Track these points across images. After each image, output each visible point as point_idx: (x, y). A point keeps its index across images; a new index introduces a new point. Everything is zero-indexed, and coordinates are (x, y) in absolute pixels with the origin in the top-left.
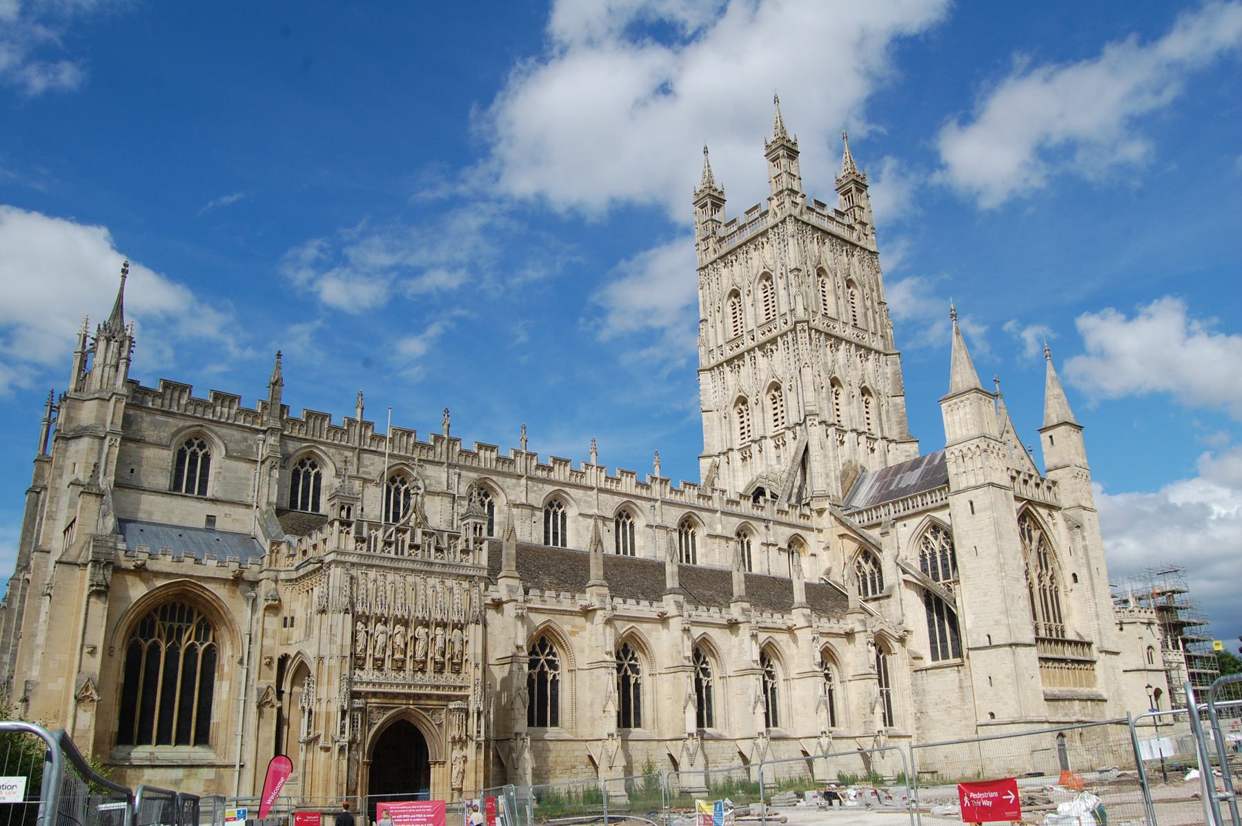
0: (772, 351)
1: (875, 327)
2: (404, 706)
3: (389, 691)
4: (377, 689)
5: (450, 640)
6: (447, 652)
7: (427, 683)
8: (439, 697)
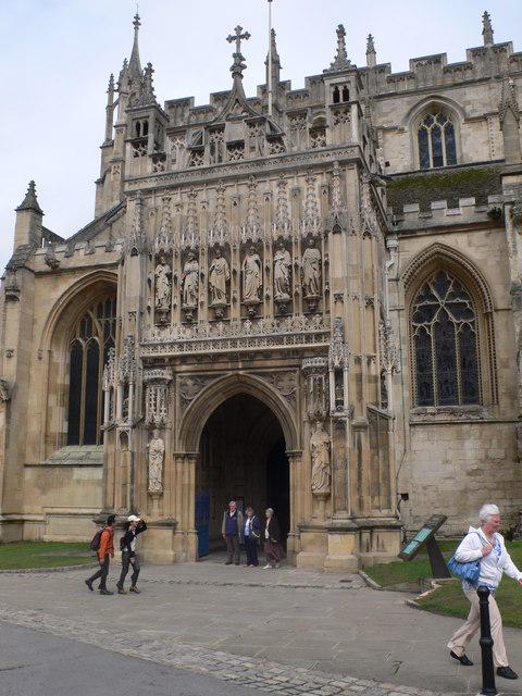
2: (230, 373)
3: (203, 352)
6: (294, 282)
7: (261, 334)
8: (285, 354)
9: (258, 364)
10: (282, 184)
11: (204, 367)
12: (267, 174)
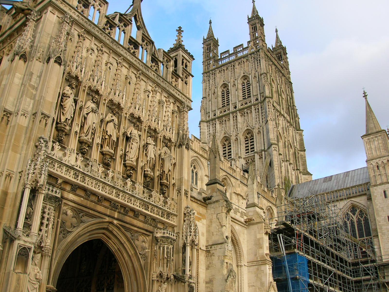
0: (247, 113)
1: (292, 116)
2: (107, 219)
3: (93, 188)
4: (79, 181)
5: (160, 155)
9: (128, 219)
10: (154, 91)
11: (88, 203)
12: (148, 78)
